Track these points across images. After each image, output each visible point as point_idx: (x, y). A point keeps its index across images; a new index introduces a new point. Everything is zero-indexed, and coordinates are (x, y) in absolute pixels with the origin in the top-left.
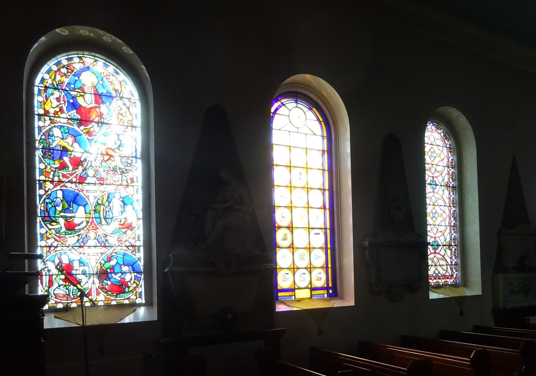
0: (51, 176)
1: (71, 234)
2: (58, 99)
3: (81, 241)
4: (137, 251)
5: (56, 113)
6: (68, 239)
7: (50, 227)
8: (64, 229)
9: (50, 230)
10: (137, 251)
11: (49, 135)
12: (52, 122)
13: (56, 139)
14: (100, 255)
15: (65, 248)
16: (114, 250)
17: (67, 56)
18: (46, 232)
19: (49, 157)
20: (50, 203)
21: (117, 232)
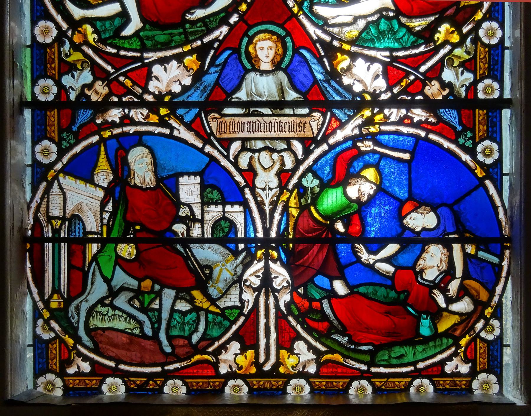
1: (166, 46)
3: (210, 79)
4: (481, 129)
6: (157, 69)
7: (77, 13)
8: (135, 23)
9: (75, 24)
10: (481, 129)
14: (298, 147)
15: (138, 114)
16: (369, 122)
18: (60, 39)
21: (382, 35)
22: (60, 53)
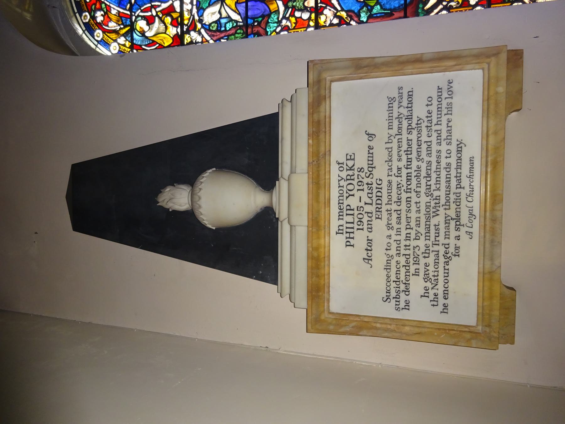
0: (305, 16)
2: (150, 21)
5: (175, 23)
11: (218, 30)
12: (192, 27)
13: (224, 14)
17: (75, 14)
19: (263, 25)
20: (370, 9)
22: (456, 8)
